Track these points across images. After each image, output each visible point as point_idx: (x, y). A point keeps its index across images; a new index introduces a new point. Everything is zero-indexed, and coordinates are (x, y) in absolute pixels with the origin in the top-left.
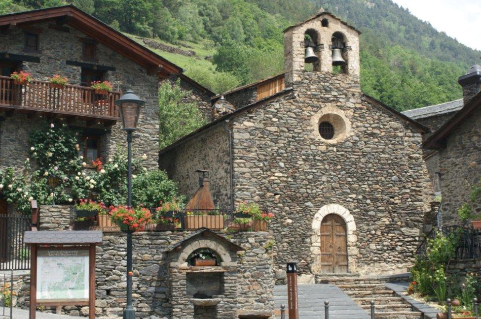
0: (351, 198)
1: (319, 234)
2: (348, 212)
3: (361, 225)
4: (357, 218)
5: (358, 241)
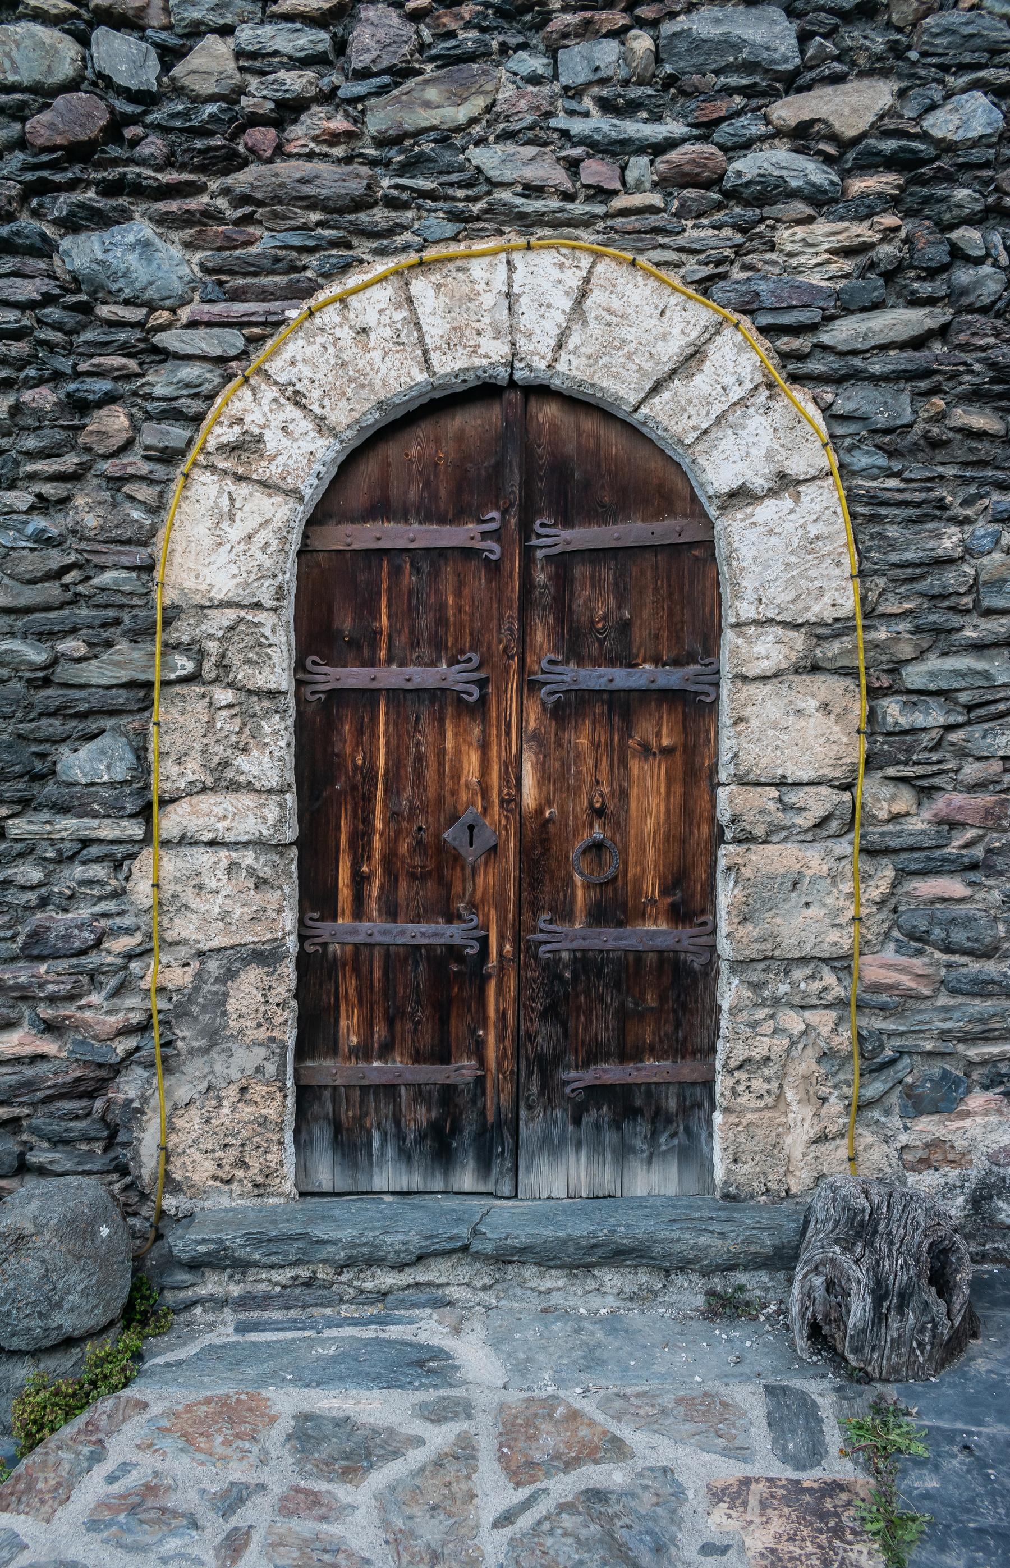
0: (802, 136)
1: (277, 674)
2: (737, 358)
3: (949, 540)
4: (889, 439)
5: (872, 763)
